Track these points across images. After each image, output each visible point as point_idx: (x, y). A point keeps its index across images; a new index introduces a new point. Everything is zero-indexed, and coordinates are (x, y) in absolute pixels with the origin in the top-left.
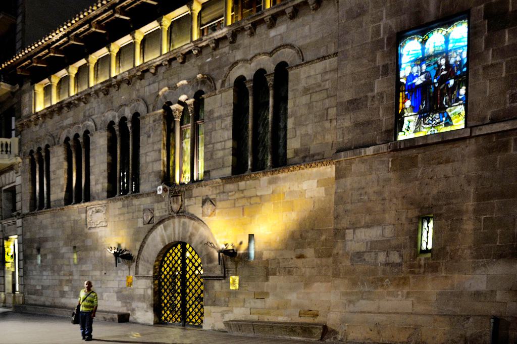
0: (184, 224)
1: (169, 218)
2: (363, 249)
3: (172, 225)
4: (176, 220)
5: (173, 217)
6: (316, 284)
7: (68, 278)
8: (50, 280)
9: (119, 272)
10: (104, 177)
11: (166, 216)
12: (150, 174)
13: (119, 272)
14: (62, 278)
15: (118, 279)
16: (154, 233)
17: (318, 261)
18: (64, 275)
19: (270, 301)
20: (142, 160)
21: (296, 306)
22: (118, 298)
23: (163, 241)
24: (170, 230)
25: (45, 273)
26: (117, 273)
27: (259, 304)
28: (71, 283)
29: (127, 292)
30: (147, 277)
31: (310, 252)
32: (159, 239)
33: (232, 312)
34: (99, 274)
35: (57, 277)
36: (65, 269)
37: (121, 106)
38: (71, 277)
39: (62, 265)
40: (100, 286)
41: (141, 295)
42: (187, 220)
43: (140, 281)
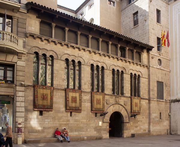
0: (119, 106)
1: (115, 104)
2: (154, 117)
3: (116, 106)
4: (117, 105)
5: (116, 104)
6: (146, 124)
7: (66, 123)
8: (51, 124)
9: (96, 120)
10: (89, 83)
11: (114, 103)
12: (108, 88)
13: (96, 120)
14: (61, 123)
15: (95, 123)
16: (110, 107)
17: (146, 119)
18: (63, 121)
19: (138, 128)
20: (105, 83)
21: (143, 129)
22: (94, 130)
23: (113, 111)
24: (115, 108)
25: (47, 120)
26: (95, 121)
27: (136, 129)
28: (68, 125)
29: (99, 128)
30: (107, 122)
31: (144, 117)
32: (111, 110)
33: (131, 131)
34: (86, 121)
35: (58, 123)
36: (64, 118)
37: (98, 61)
38: (68, 122)
39: (62, 117)
40: (86, 126)
41: (105, 129)
42: (120, 106)
43: (105, 124)
